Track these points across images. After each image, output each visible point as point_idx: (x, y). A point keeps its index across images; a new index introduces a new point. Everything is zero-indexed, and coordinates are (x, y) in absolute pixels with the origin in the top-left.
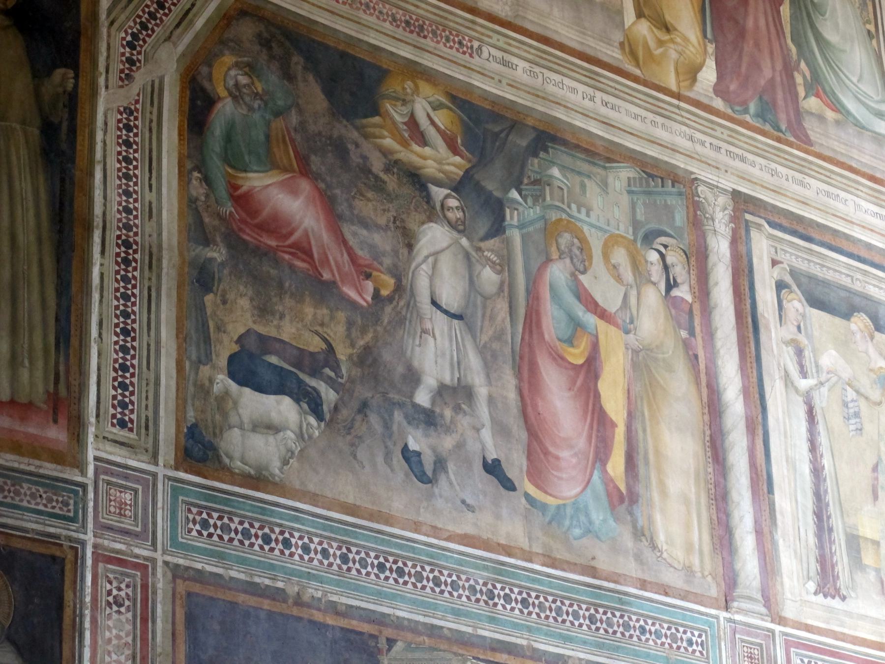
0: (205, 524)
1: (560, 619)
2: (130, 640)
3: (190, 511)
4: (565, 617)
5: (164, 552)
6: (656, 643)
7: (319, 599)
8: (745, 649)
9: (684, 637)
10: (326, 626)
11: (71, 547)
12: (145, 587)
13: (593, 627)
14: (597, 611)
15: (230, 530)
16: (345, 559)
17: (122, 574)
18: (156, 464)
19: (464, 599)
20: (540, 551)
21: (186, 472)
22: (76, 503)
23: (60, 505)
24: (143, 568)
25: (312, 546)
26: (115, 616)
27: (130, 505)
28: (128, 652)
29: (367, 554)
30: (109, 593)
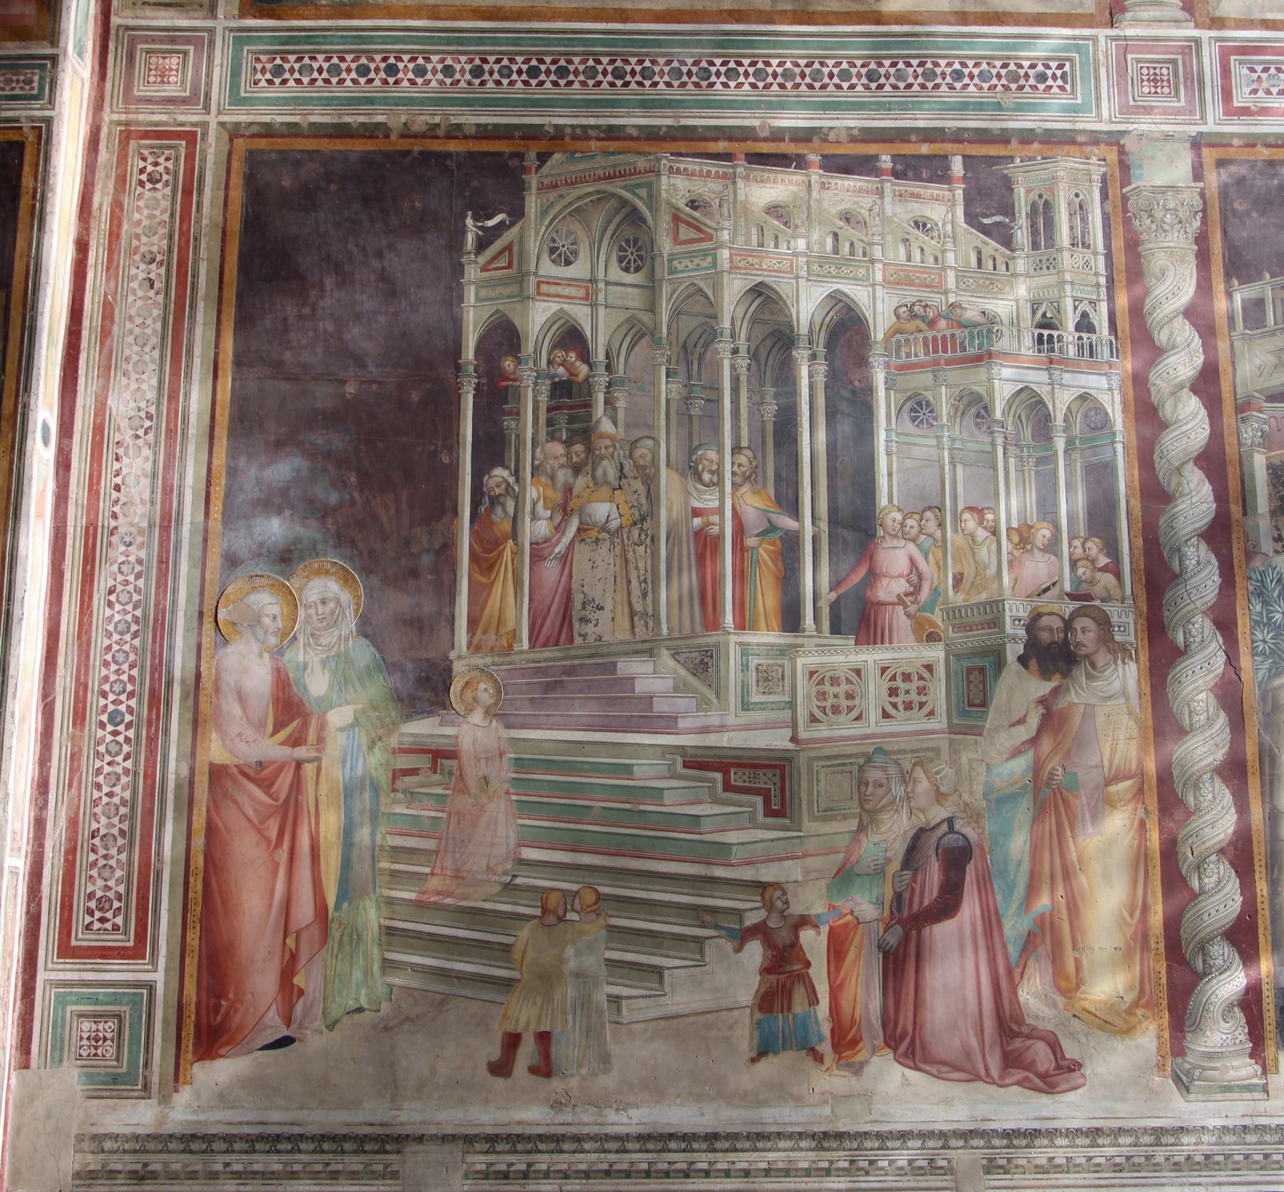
0: (278, 71)
1: (817, 85)
2: (166, 217)
3: (258, 60)
4: (826, 80)
5: (219, 113)
6: (981, 88)
7: (438, 125)
8: (1145, 71)
9: (1031, 72)
10: (448, 155)
11: (33, 128)
12: (190, 157)
13: (873, 85)
14: (880, 65)
15: (312, 69)
16: (477, 72)
17: (161, 147)
18: (215, 17)
19: (661, 86)
20: (789, 7)
21: (255, 17)
22: (42, 79)
23: (22, 85)
24: (190, 138)
25: (429, 67)
26: (148, 194)
27: (177, 70)
28: (163, 231)
29: (512, 61)
30: (142, 171)
